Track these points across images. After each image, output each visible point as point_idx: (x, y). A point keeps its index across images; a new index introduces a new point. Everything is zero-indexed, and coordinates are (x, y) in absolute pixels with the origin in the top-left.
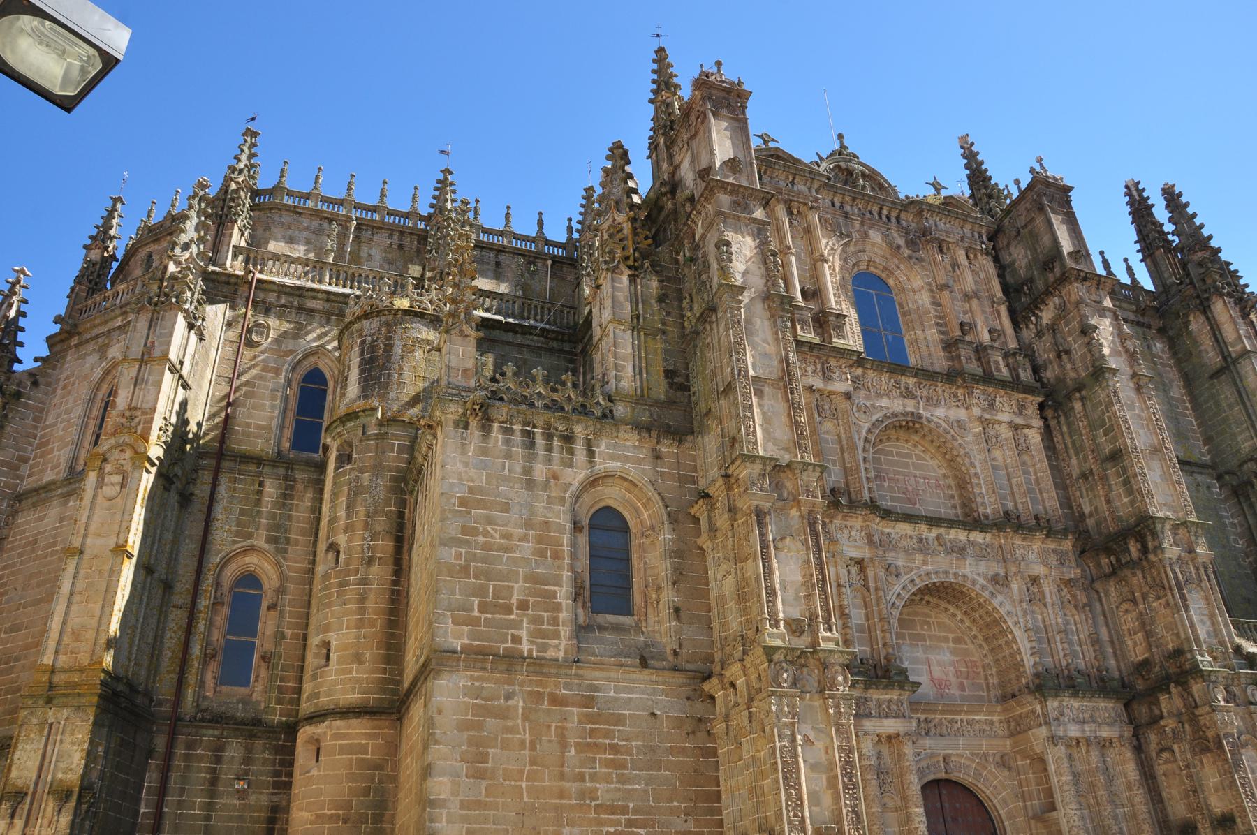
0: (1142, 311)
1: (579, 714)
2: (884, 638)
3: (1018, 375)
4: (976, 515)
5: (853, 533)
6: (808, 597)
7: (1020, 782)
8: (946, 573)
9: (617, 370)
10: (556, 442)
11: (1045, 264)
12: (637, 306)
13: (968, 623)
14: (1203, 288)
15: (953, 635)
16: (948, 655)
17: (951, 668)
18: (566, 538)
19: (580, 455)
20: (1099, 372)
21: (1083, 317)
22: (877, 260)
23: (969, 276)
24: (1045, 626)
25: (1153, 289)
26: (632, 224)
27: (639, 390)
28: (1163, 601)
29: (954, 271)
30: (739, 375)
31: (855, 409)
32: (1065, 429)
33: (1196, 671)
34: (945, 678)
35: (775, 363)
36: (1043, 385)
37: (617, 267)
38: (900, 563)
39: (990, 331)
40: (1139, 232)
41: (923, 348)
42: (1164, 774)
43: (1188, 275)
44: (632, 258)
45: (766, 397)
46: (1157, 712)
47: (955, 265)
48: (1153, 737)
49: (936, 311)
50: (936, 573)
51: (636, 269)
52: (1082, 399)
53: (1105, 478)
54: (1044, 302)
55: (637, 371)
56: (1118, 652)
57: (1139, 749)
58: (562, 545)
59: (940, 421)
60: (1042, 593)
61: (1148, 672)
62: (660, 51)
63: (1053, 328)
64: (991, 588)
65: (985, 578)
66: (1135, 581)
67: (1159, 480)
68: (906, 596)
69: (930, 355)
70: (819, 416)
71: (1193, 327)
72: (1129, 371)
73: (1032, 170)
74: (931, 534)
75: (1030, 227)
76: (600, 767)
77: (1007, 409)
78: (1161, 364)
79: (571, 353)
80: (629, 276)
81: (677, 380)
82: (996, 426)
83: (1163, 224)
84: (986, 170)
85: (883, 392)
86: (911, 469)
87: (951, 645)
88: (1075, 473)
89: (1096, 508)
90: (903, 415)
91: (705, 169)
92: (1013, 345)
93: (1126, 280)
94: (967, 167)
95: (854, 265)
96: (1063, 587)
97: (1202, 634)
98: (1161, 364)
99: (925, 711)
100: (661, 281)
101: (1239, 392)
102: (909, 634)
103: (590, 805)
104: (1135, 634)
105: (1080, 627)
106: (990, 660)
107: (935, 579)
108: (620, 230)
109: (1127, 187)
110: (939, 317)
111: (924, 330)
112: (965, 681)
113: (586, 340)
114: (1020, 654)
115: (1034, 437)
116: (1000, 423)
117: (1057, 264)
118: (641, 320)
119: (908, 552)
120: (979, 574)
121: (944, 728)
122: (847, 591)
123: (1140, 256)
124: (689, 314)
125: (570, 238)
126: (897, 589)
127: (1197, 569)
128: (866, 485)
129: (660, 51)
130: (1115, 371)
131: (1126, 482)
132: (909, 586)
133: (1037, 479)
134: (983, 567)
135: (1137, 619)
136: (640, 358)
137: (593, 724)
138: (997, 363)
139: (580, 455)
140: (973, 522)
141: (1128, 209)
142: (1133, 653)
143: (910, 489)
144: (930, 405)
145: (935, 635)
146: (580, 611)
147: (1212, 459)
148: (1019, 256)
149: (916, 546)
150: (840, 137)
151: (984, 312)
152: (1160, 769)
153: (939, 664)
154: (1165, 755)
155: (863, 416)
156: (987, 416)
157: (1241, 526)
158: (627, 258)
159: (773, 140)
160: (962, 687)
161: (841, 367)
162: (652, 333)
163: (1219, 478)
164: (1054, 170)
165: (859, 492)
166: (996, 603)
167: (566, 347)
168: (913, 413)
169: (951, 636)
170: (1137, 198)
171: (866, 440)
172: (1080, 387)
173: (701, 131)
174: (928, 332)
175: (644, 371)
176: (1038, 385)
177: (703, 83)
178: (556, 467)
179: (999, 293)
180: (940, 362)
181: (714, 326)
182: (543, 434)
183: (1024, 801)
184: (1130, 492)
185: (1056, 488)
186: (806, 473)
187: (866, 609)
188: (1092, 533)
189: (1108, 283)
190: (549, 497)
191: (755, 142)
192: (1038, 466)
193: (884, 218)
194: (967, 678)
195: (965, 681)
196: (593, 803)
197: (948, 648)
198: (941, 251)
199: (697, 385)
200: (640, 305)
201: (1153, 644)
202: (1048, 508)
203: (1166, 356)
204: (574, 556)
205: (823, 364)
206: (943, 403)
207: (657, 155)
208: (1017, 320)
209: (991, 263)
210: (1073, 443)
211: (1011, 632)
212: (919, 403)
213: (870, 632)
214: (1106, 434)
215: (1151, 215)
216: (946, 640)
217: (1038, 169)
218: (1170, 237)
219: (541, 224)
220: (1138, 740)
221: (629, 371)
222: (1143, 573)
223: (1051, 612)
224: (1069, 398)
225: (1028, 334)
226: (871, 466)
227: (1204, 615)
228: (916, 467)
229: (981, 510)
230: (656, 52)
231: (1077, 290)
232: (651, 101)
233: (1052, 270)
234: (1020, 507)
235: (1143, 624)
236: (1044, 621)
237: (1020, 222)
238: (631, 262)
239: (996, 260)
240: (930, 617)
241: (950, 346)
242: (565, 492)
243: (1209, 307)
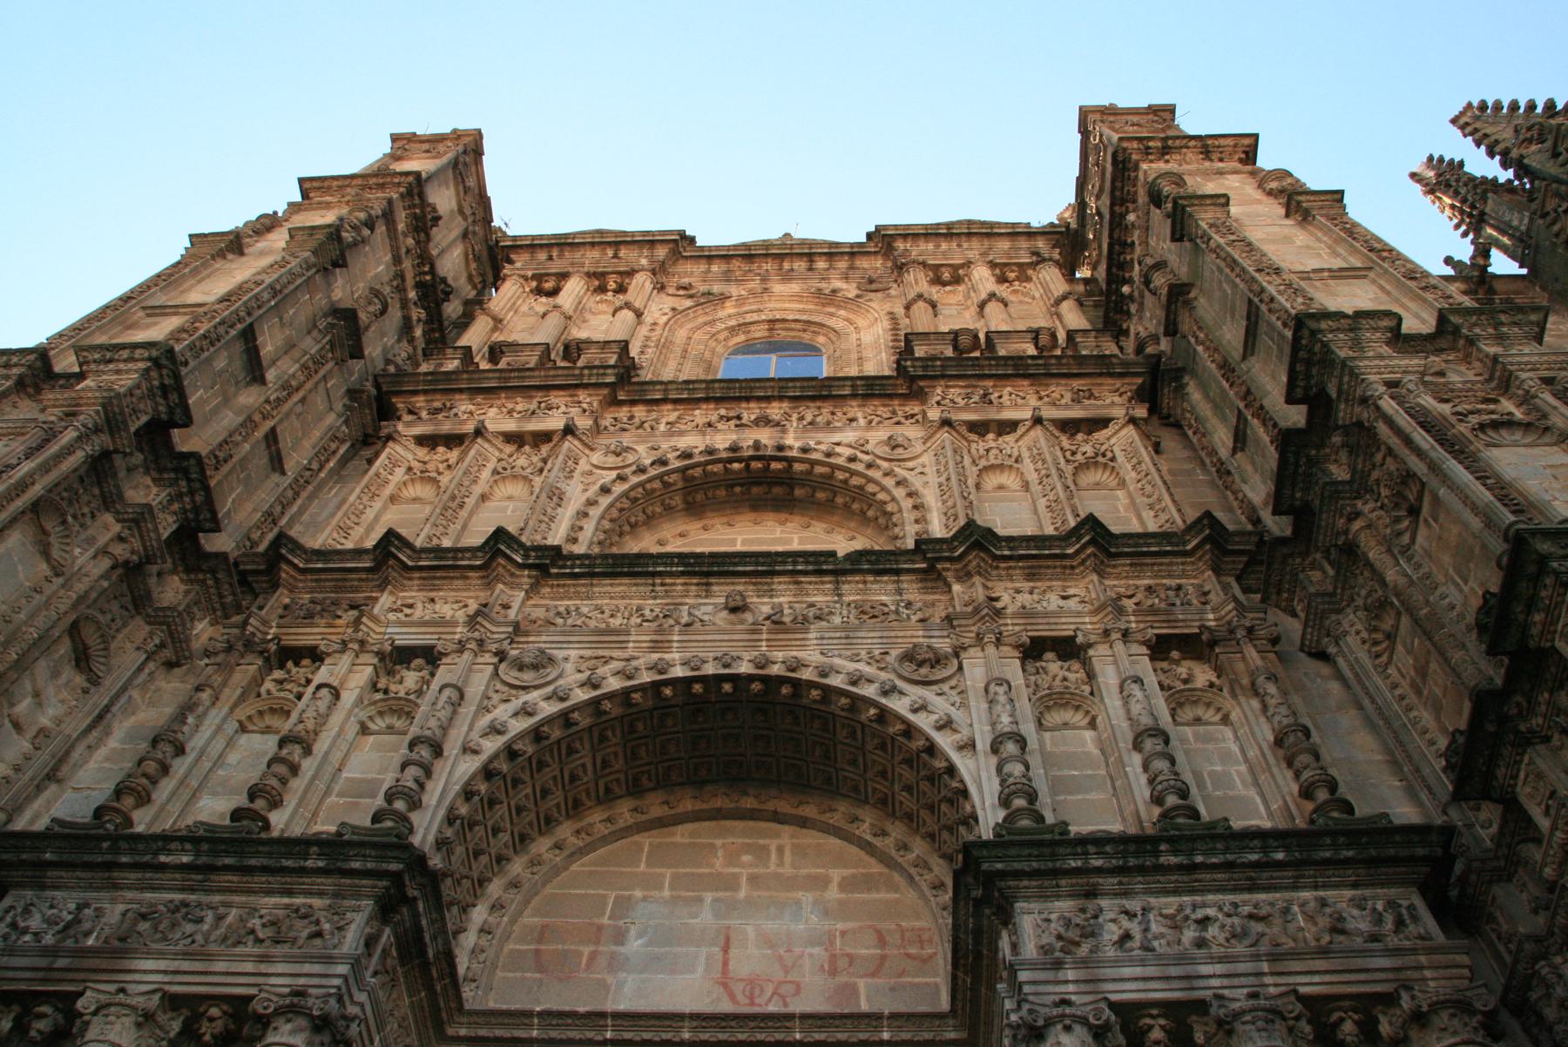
13: (897, 831)
15: (847, 872)
60: (1091, 676)
65: (879, 661)
87: (833, 893)
95: (733, 330)
102: (675, 877)
134: (870, 639)
145: (777, 876)
153: (768, 941)
166: (899, 705)
169: (836, 874)
192: (1130, 476)
194: (873, 975)
195: (862, 984)
197: (815, 903)
216: (821, 883)
240: (777, 835)
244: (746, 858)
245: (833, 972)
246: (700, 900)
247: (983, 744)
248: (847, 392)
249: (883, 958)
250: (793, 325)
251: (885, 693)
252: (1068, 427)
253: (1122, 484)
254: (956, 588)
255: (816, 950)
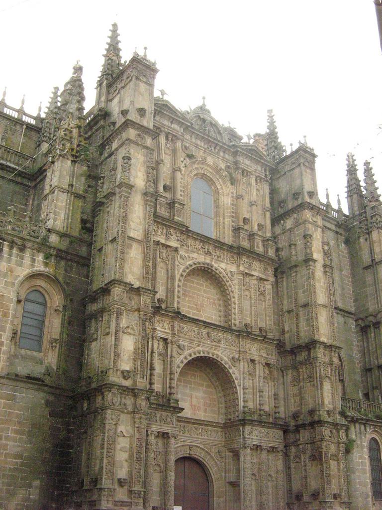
0: (338, 225)
1: (5, 404)
2: (170, 383)
3: (267, 253)
4: (230, 323)
5: (165, 324)
6: (135, 360)
7: (225, 463)
8: (208, 353)
9: (55, 215)
10: (15, 251)
11: (294, 194)
12: (73, 179)
14: (372, 221)
16: (202, 393)
17: (202, 400)
18: (12, 306)
19: (27, 261)
20: (308, 260)
21: (306, 229)
22: (208, 174)
23: (254, 192)
24: (253, 386)
25: (348, 214)
26: (79, 129)
27: (65, 229)
28: (312, 383)
29: (247, 188)
30: (121, 235)
31: (179, 257)
32: (285, 283)
33: (320, 422)
34: (198, 405)
35: (141, 231)
36: (279, 259)
37: (65, 154)
38: (186, 344)
39: (258, 225)
40: (348, 182)
41: (221, 228)
42: (295, 468)
43: (365, 212)
44: (75, 151)
45: (133, 249)
46: (298, 437)
47: (249, 184)
48: (293, 449)
49: (233, 208)
50: (204, 353)
51: (77, 157)
52: (296, 272)
53: (297, 315)
54: (289, 215)
55: (66, 217)
56: (286, 405)
57: (286, 455)
58: (9, 309)
59: (222, 270)
60: (255, 368)
61: (298, 417)
62: (115, 25)
63: (291, 230)
64: (230, 363)
65: (228, 358)
66: (301, 370)
67: (323, 321)
68: (185, 361)
69: (224, 232)
70: (160, 258)
71: (362, 240)
72: (323, 262)
73: (300, 143)
74: (204, 331)
75: (292, 172)
76: (11, 433)
77: (258, 269)
78: (343, 256)
79: (26, 186)
80: (72, 161)
81: (88, 225)
82: (250, 277)
83: (360, 181)
84: (277, 133)
85: (195, 250)
86: (202, 293)
87: (204, 388)
88: (285, 308)
89: (291, 329)
90: (204, 264)
91: (125, 110)
92: (269, 235)
93: (335, 206)
94: (269, 128)
96: (266, 367)
97: (326, 402)
98: (343, 256)
99: (184, 422)
100: (88, 167)
101: (375, 279)
102: (184, 380)
103: (2, 453)
104: (296, 397)
105: (269, 390)
106: (223, 400)
107: (202, 354)
108: (71, 132)
109: (348, 156)
110: (233, 212)
111: (224, 218)
112: (208, 408)
113: (38, 180)
114: (237, 399)
115: (268, 287)
116: (252, 276)
117: (300, 197)
118: (74, 188)
119: (191, 341)
120: (225, 356)
121: (192, 431)
122: (156, 355)
123: (346, 195)
124: (100, 190)
125: (39, 115)
126: (182, 357)
127: (332, 370)
128: (176, 299)
129: (115, 25)
130: (315, 261)
131: (308, 320)
132: (188, 357)
133: (265, 308)
135: (298, 390)
136: (69, 209)
137: (11, 409)
138: (258, 244)
139: (27, 261)
140: (227, 329)
141: (346, 168)
142: (293, 406)
143: (199, 303)
144: (219, 260)
146: (13, 346)
147: (355, 310)
148: (283, 186)
149: (196, 336)
150: (204, 98)
151: (257, 213)
152: (293, 466)
154: (298, 460)
155: (183, 261)
156: (247, 271)
157: (361, 347)
158: (72, 150)
159: (166, 94)
160: (205, 411)
161: (176, 233)
162: (77, 196)
163: (356, 321)
164: (310, 145)
165: (172, 303)
166: (231, 371)
167: (26, 182)
168: (208, 265)
169: (205, 383)
170: (351, 163)
171: (182, 275)
172: (296, 266)
173: (128, 86)
174: (226, 220)
175: (70, 218)
176: (276, 259)
177: (135, 60)
178: (13, 265)
179: (268, 205)
180: (228, 239)
181: (113, 203)
182: (9, 245)
183: (225, 473)
184: (308, 325)
185: (274, 315)
186: (146, 294)
187: (164, 366)
188: (286, 341)
189: (324, 211)
190: (6, 281)
191: (157, 94)
192: (267, 302)
193: (217, 150)
195: (208, 408)
196: (4, 452)
197: (203, 389)
198: (243, 175)
199: (98, 232)
200: (75, 179)
201: (303, 404)
202: (268, 325)
203: (346, 251)
204: (14, 316)
205: (167, 230)
206: (225, 260)
207: (100, 89)
208: (275, 221)
209: (268, 187)
210: (288, 292)
211: (236, 387)
212: (213, 259)
213: (163, 378)
214: (304, 292)
215: (355, 174)
216: (202, 385)
217: (303, 142)
218: (362, 189)
219: (23, 102)
220: (286, 450)
221: (62, 216)
222: (307, 368)
223: (257, 379)
224: (291, 268)
225: (278, 230)
226: (180, 290)
227: (329, 393)
228: (205, 291)
229: (233, 321)
230: (113, 25)
231: (308, 214)
232: (104, 56)
233: (297, 199)
234: (253, 322)
235: (300, 393)
236: (253, 383)
237: (287, 168)
238: (74, 153)
239: (271, 185)
241: (237, 230)
242: (15, 280)
243: (371, 232)
244: (193, 377)
245: (204, 405)
246: (187, 386)
247: (242, 386)
248: (226, 248)
249: (210, 404)
250: (208, 177)
251: (229, 368)
252: (261, 279)
253: (265, 301)
254: (241, 339)
255: (202, 400)
